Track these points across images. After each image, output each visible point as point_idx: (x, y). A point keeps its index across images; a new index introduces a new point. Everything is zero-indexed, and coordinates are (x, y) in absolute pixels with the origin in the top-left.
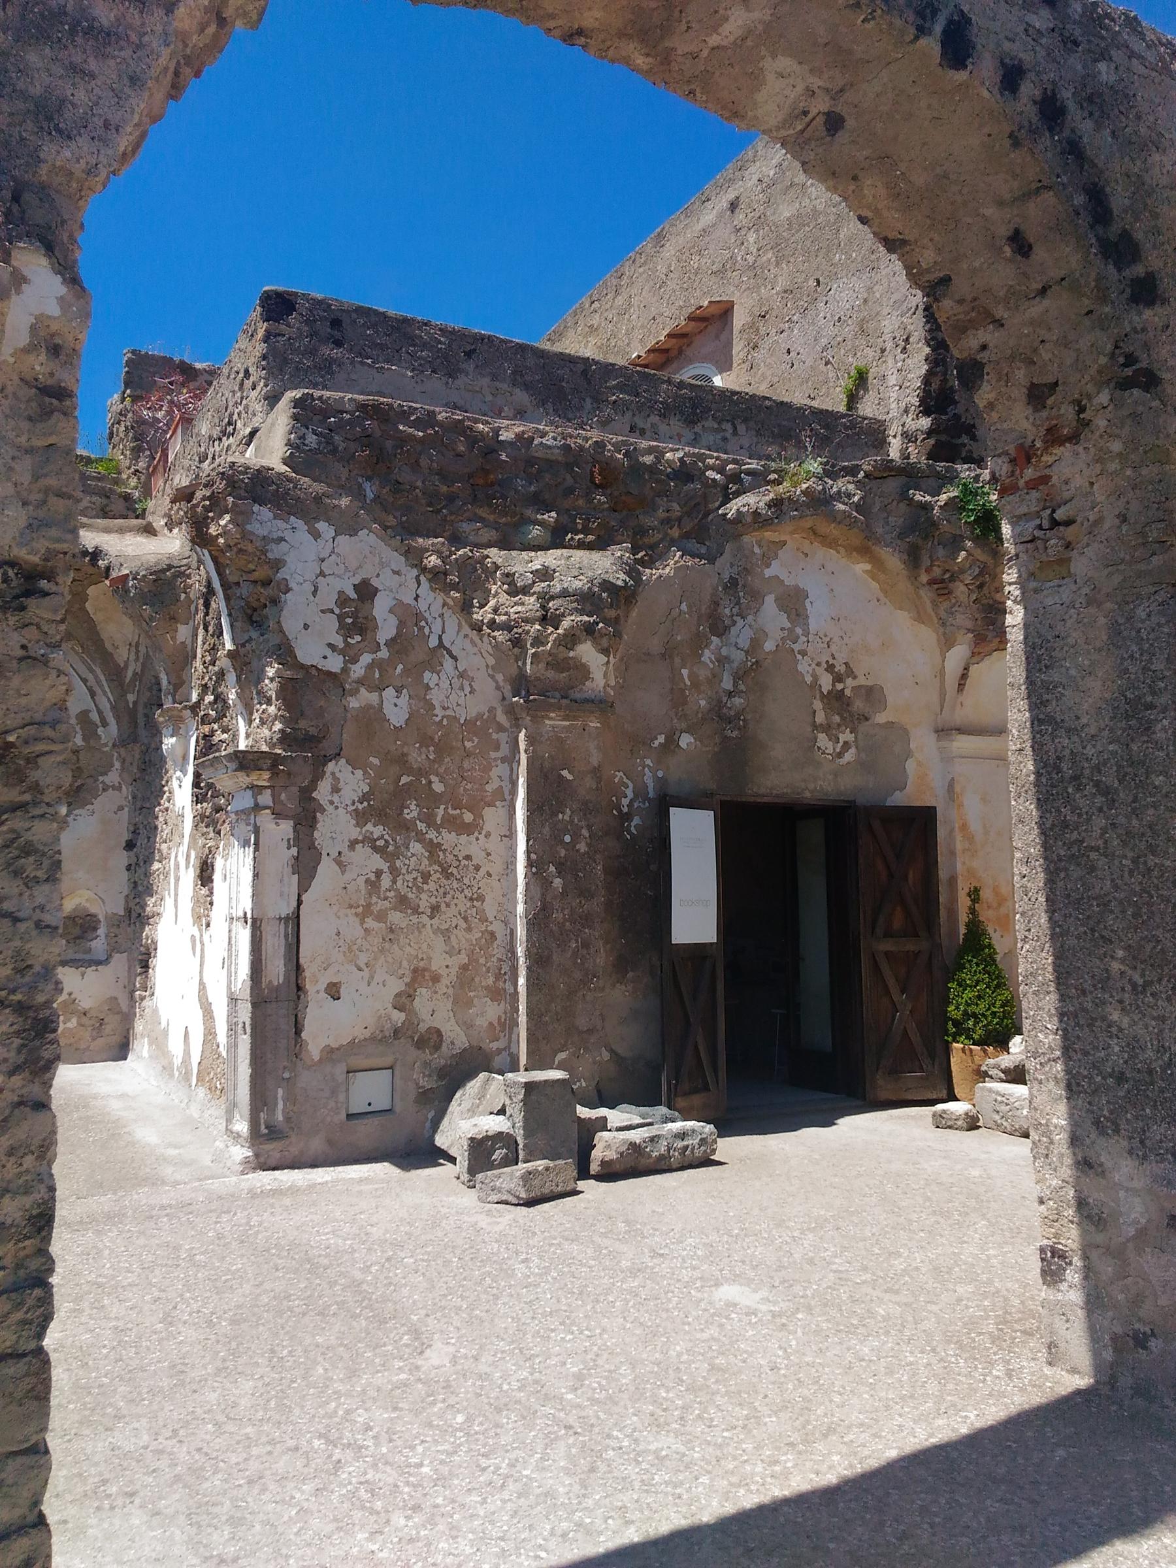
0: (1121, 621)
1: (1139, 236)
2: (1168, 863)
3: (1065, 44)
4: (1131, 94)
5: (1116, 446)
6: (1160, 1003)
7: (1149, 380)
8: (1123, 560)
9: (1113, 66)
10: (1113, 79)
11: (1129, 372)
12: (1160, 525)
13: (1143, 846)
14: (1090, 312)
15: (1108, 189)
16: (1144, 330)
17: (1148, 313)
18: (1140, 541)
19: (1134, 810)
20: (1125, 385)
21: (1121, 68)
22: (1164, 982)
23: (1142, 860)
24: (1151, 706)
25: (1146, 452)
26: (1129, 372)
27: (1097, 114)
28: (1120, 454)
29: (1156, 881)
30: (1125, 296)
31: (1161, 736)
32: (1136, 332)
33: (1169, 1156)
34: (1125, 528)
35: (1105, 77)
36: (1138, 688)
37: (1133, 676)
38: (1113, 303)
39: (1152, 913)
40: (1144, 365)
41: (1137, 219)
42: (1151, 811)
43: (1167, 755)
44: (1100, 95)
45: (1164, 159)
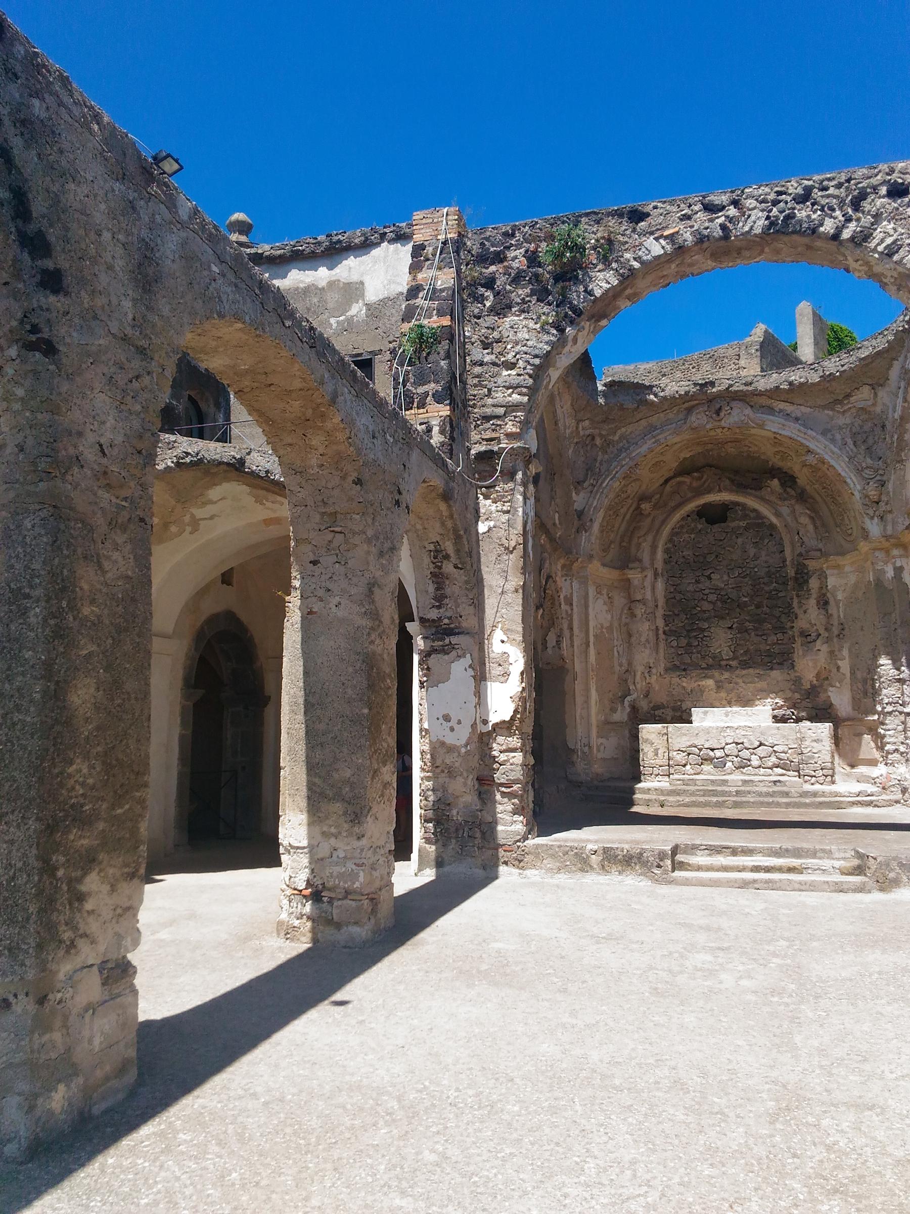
0: (12, 527)
1: (52, 239)
2: (28, 719)
3: (7, 73)
4: (57, 132)
5: (20, 392)
6: (12, 829)
7: (49, 349)
8: (17, 481)
9: (44, 105)
10: (43, 115)
11: (33, 338)
12: (49, 460)
13: (11, 705)
14: (6, 284)
15: (30, 196)
16: (48, 310)
17: (52, 299)
18: (32, 468)
19: (8, 676)
20: (30, 347)
21: (51, 110)
22: (16, 813)
23: (9, 716)
24: (27, 596)
25: (42, 402)
26: (33, 338)
27: (27, 136)
28: (22, 399)
29: (18, 733)
30: (35, 280)
31: (33, 620)
32: (42, 310)
33: (6, 952)
34: (21, 457)
35: (37, 110)
36: (20, 581)
37: (17, 572)
38: (24, 281)
39: (13, 758)
40: (46, 336)
41: (51, 226)
42: (20, 678)
43: (37, 635)
44: (32, 123)
45: (79, 190)
